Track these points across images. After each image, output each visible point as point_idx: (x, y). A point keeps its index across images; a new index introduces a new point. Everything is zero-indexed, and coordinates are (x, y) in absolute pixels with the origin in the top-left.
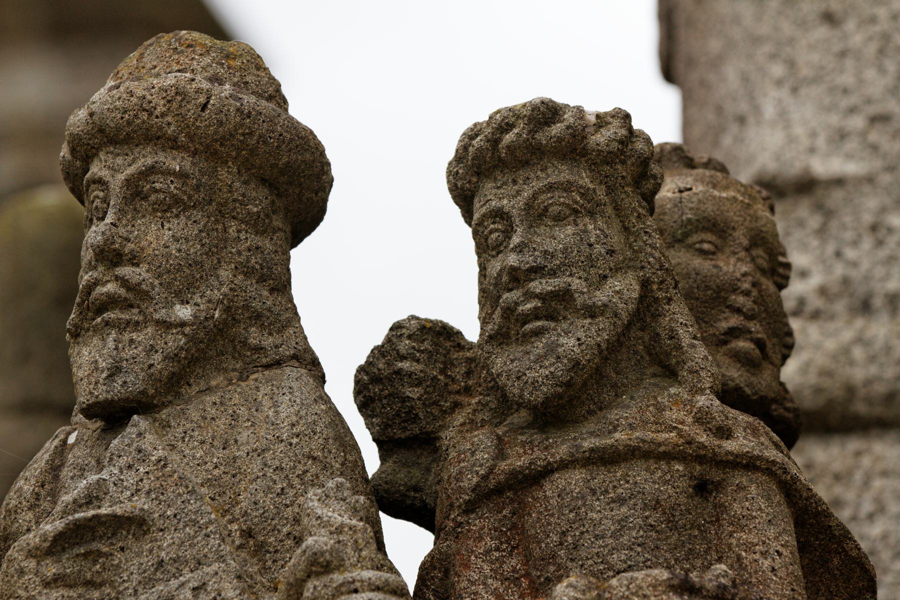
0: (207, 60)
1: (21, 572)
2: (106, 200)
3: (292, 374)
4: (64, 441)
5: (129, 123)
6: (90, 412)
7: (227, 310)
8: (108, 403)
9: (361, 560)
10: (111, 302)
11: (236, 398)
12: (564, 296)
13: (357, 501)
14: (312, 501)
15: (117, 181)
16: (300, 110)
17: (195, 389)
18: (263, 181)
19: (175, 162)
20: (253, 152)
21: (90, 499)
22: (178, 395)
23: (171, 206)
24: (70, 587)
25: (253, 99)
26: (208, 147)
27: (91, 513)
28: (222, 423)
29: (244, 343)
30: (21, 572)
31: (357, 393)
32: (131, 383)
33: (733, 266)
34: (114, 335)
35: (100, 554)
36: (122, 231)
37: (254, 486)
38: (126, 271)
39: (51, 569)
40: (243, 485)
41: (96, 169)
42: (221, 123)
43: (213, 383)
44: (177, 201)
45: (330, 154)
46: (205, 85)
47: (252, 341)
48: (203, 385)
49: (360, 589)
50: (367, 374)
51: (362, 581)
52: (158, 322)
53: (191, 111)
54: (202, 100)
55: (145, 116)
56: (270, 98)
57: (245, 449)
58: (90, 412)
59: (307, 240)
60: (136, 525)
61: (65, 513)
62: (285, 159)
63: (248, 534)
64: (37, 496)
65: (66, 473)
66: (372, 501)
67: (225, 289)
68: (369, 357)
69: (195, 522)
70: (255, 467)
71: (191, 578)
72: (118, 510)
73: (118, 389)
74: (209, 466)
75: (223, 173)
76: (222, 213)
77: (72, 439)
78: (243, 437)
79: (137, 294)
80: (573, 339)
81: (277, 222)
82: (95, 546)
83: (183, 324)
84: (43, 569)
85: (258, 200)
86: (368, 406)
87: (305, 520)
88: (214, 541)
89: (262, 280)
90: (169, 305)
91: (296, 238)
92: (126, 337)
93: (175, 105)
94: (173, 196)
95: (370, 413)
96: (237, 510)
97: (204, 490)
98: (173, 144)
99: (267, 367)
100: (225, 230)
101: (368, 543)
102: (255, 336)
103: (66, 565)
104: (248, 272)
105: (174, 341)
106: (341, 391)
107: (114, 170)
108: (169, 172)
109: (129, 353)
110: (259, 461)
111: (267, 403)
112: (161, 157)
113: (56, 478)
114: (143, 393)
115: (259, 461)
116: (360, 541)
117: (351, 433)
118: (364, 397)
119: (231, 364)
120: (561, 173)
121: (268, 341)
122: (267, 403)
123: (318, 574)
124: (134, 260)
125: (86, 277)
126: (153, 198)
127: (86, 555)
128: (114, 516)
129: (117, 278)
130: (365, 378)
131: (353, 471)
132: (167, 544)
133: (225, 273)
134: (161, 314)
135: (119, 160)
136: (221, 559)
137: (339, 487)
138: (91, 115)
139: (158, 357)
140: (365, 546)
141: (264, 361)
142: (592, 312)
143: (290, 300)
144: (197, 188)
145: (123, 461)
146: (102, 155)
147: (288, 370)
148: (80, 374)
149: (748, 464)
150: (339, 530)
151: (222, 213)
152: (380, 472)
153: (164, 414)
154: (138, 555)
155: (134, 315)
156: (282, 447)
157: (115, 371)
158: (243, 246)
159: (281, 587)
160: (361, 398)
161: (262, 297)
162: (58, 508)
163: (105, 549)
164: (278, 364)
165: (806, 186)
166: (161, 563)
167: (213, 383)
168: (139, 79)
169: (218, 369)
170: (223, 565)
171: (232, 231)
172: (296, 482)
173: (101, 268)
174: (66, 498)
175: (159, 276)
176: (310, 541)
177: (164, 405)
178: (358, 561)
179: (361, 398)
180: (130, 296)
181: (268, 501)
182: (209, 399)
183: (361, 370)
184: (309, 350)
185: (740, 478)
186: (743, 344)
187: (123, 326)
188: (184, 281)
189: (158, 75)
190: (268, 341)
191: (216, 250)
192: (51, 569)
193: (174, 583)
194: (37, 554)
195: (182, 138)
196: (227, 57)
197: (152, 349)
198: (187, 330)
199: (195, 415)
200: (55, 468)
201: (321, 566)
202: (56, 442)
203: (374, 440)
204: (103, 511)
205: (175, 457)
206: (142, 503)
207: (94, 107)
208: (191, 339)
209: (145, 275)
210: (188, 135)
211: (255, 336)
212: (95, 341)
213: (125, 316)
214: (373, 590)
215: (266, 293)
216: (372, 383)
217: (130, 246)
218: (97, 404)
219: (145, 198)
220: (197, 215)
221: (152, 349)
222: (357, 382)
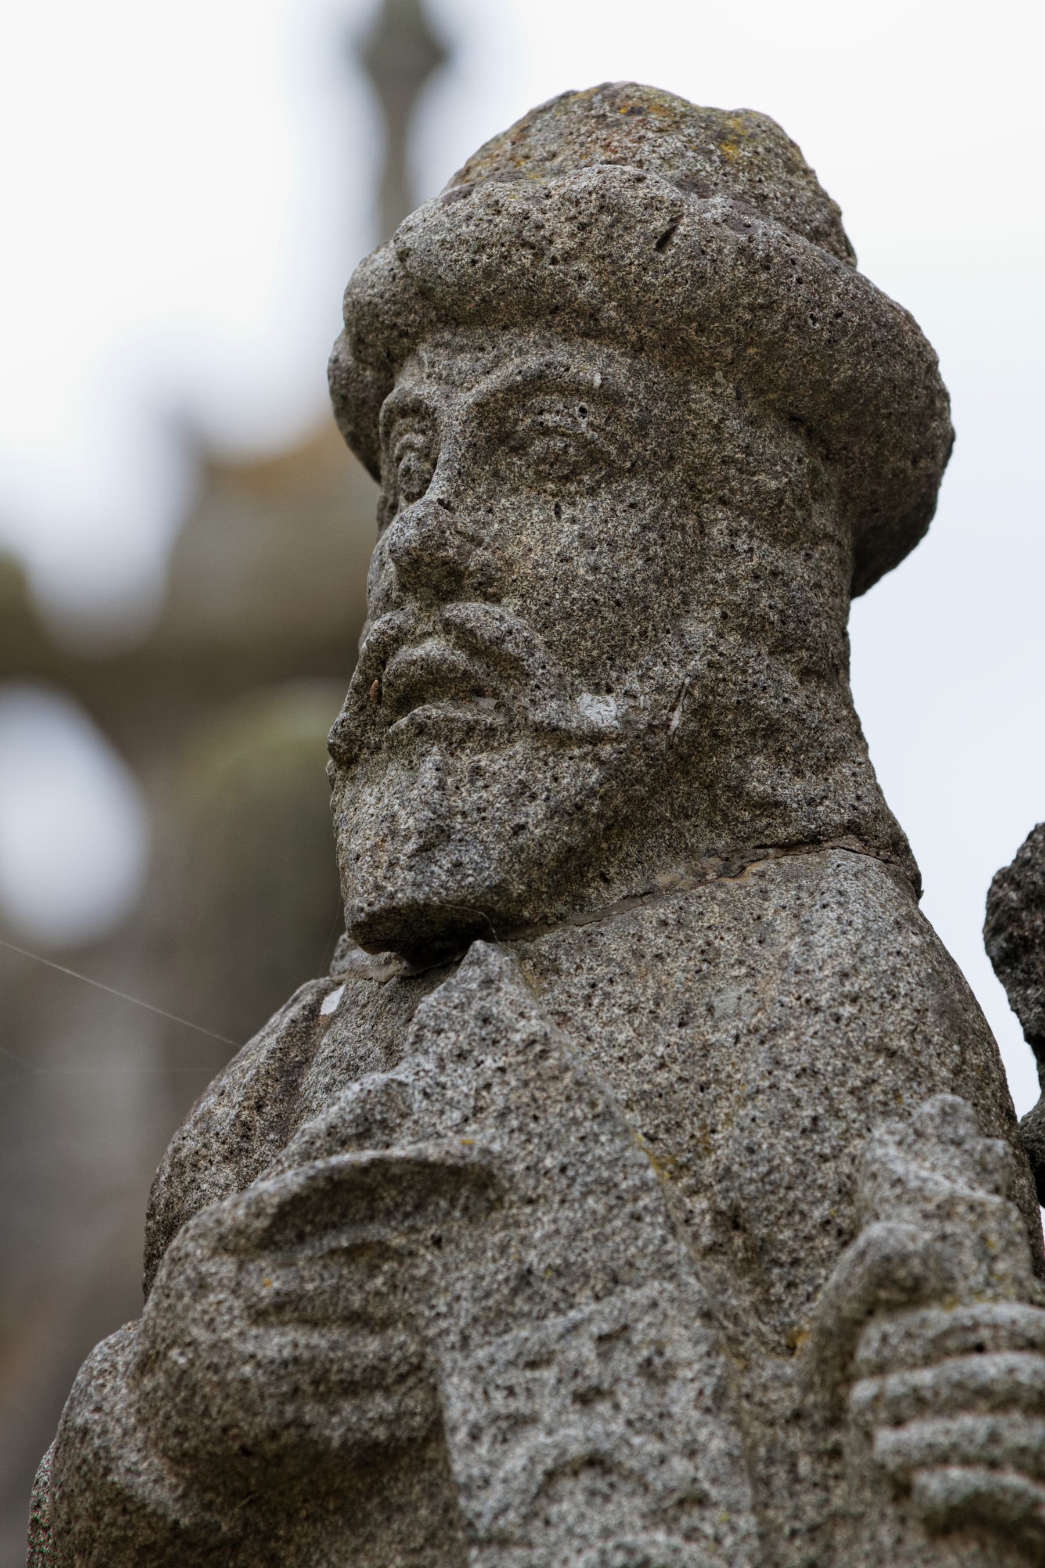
0: (674, 142)
1: (201, 1286)
2: (428, 455)
3: (844, 867)
4: (313, 1010)
5: (489, 274)
6: (374, 933)
7: (701, 711)
8: (419, 911)
9: (993, 1280)
10: (433, 682)
11: (714, 914)
13: (989, 1149)
14: (884, 1145)
15: (455, 409)
16: (887, 260)
17: (619, 889)
18: (794, 421)
19: (592, 367)
20: (772, 349)
21: (366, 1127)
22: (579, 902)
23: (577, 469)
24: (314, 1324)
25: (777, 230)
26: (669, 333)
27: (367, 1155)
28: (679, 968)
29: (737, 792)
30: (201, 1286)
31: (992, 931)
32: (474, 866)
34: (436, 754)
35: (384, 1251)
36: (464, 520)
37: (749, 1110)
38: (469, 610)
39: (269, 1281)
40: (723, 1109)
41: (410, 384)
42: (701, 279)
43: (662, 879)
44: (593, 456)
45: (949, 374)
46: (668, 192)
47: (756, 787)
48: (638, 884)
49: (990, 1344)
50: (1018, 886)
51: (995, 1326)
52: (538, 730)
53: (633, 247)
54: (659, 223)
55: (526, 257)
56: (816, 236)
57: (732, 1026)
58: (379, 932)
59: (888, 581)
60: (470, 1187)
61: (306, 1156)
62: (845, 372)
63: (732, 1220)
64: (246, 1130)
65: (314, 1077)
66: (1020, 1162)
67: (696, 664)
68: (1022, 849)
69: (608, 1186)
70: (754, 1068)
71: (596, 1313)
72: (432, 1151)
73: (438, 882)
74: (647, 1063)
75: (701, 397)
76: (696, 491)
77: (330, 1005)
78: (727, 1001)
79: (493, 664)
81: (822, 519)
82: (374, 1232)
83: (596, 737)
84: (251, 1281)
85: (780, 462)
86: (1018, 959)
87: (866, 1189)
88: (652, 1231)
89: (782, 647)
90: (567, 693)
91: (865, 573)
92: (465, 761)
93: (596, 235)
94: (585, 444)
95: (1021, 976)
96: (708, 1166)
97: (631, 1117)
98: (589, 326)
99: (788, 847)
100: (702, 530)
101: (1011, 1243)
102: (761, 776)
103: (306, 1273)
104: (752, 628)
105: (575, 775)
106: (957, 914)
107: (452, 383)
108: (577, 389)
109: (469, 798)
110: (763, 1053)
111: (784, 925)
112: (560, 354)
113: (292, 1089)
114: (499, 889)
115: (763, 1053)
116: (993, 1238)
117: (978, 1007)
118: (1010, 939)
119: (703, 839)
121: (792, 789)
122: (784, 925)
123: (892, 1308)
124: (489, 588)
125: (377, 625)
126: (538, 447)
127: (352, 1253)
128: (422, 1165)
129: (448, 626)
130: (1013, 895)
131: (979, 1088)
132: (542, 1234)
133: (698, 628)
134: (548, 712)
135: (464, 362)
136: (667, 1271)
137: (947, 1114)
138: (403, 256)
139: (536, 810)
140: (1005, 1250)
141: (782, 833)
143: (847, 702)
144: (641, 428)
145: (445, 1043)
146: (424, 352)
147: (836, 856)
148: (356, 845)
150: (945, 1210)
151: (696, 491)
152: (1041, 1109)
153: (544, 943)
154: (474, 1256)
155: (483, 712)
156: (816, 1023)
157: (436, 837)
158: (742, 568)
159: (805, 1343)
160: (1001, 941)
161: (782, 689)
162: (293, 1147)
163: (397, 1241)
164: (813, 841)
166: (526, 1277)
167: (662, 879)
168: (515, 177)
169: (673, 850)
170: (669, 1286)
171: (718, 533)
172: (847, 1105)
173: (411, 605)
174: (315, 1124)
175: (547, 626)
176: (875, 1230)
177: (547, 923)
178: (988, 1284)
179: (1001, 941)
180: (477, 668)
181: (779, 1146)
182: (651, 913)
183: (1004, 878)
184: (883, 814)
187: (457, 738)
188: (605, 637)
189: (560, 172)
190: (792, 789)
191: (678, 574)
192: (269, 1281)
193: (555, 1323)
194: (232, 1244)
195: (611, 312)
196: (721, 137)
197: (524, 791)
198: (606, 751)
199: (617, 947)
200: (288, 1072)
201: (897, 1287)
202: (294, 1011)
203: (1028, 1038)
204: (396, 1152)
205: (567, 1039)
206: (485, 1138)
207: (409, 240)
208: (614, 772)
209: (518, 623)
210: (624, 305)
211: (761, 776)
212: (393, 771)
213: (464, 714)
214: (1019, 1348)
215: (790, 679)
216: (1027, 908)
217: (481, 555)
218: (392, 912)
219: (520, 449)
220: (639, 490)
221: (524, 791)
222: (994, 905)
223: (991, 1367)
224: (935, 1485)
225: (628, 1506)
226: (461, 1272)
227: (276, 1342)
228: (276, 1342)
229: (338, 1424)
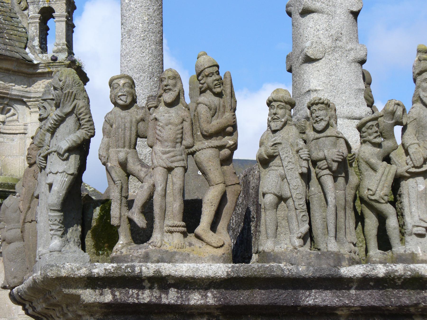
12: (322, 119)
15: (276, 106)
19: (282, 104)
21: (275, 140)
38: (277, 115)
39: (272, 148)
60: (280, 143)
120: (322, 105)
132: (283, 145)
142: (325, 121)
157: (276, 127)
181: (293, 141)
185: (340, 139)
187: (277, 121)
188: (283, 116)
224: (304, 158)
225: (289, 158)
226: (280, 147)
227: (273, 151)
228: (273, 151)
229: (275, 154)
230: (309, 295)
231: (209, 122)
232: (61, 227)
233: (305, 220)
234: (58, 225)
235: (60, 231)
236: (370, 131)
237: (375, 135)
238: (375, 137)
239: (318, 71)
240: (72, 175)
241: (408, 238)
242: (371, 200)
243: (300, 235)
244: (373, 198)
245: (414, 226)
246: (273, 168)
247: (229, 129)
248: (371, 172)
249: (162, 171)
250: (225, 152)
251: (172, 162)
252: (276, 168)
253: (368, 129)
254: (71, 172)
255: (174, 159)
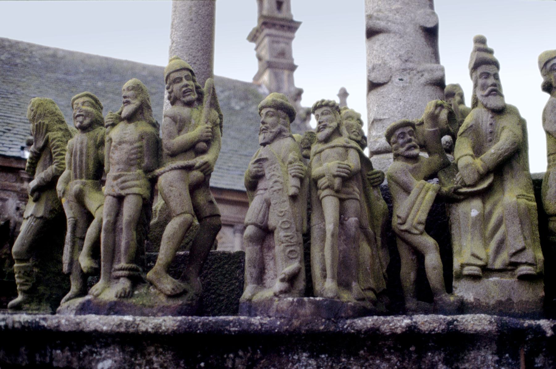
23: (272, 116)
32: (266, 140)
33: (353, 122)
38: (265, 125)
80: (327, 131)
103: (256, 165)
124: (267, 123)
142: (330, 127)
149: (351, 147)
157: (264, 138)
165: (380, 120)
186: (356, 133)
187: (265, 132)
188: (274, 126)
206: (267, 156)
223: (296, 167)
226: (265, 164)
228: (255, 169)
230: (299, 360)
231: (171, 136)
232: (27, 281)
233: (294, 256)
234: (24, 278)
235: (27, 285)
236: (401, 141)
237: (407, 145)
238: (409, 149)
239: (383, 97)
240: (41, 218)
241: (454, 283)
242: (402, 231)
243: (283, 276)
244: (404, 227)
245: (463, 266)
246: (259, 192)
247: (202, 145)
248: (402, 195)
249: (111, 201)
250: (196, 175)
251: (122, 189)
252: (261, 192)
253: (398, 137)
254: (40, 214)
255: (124, 184)
